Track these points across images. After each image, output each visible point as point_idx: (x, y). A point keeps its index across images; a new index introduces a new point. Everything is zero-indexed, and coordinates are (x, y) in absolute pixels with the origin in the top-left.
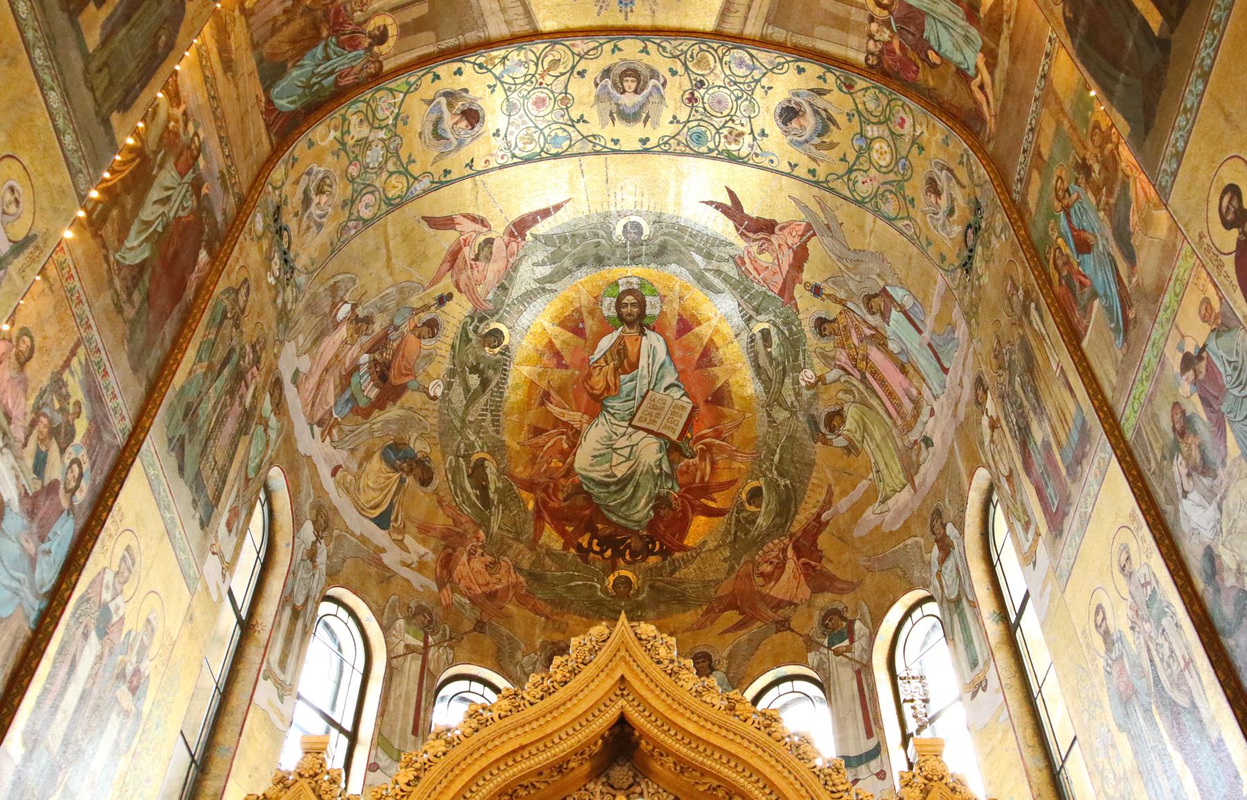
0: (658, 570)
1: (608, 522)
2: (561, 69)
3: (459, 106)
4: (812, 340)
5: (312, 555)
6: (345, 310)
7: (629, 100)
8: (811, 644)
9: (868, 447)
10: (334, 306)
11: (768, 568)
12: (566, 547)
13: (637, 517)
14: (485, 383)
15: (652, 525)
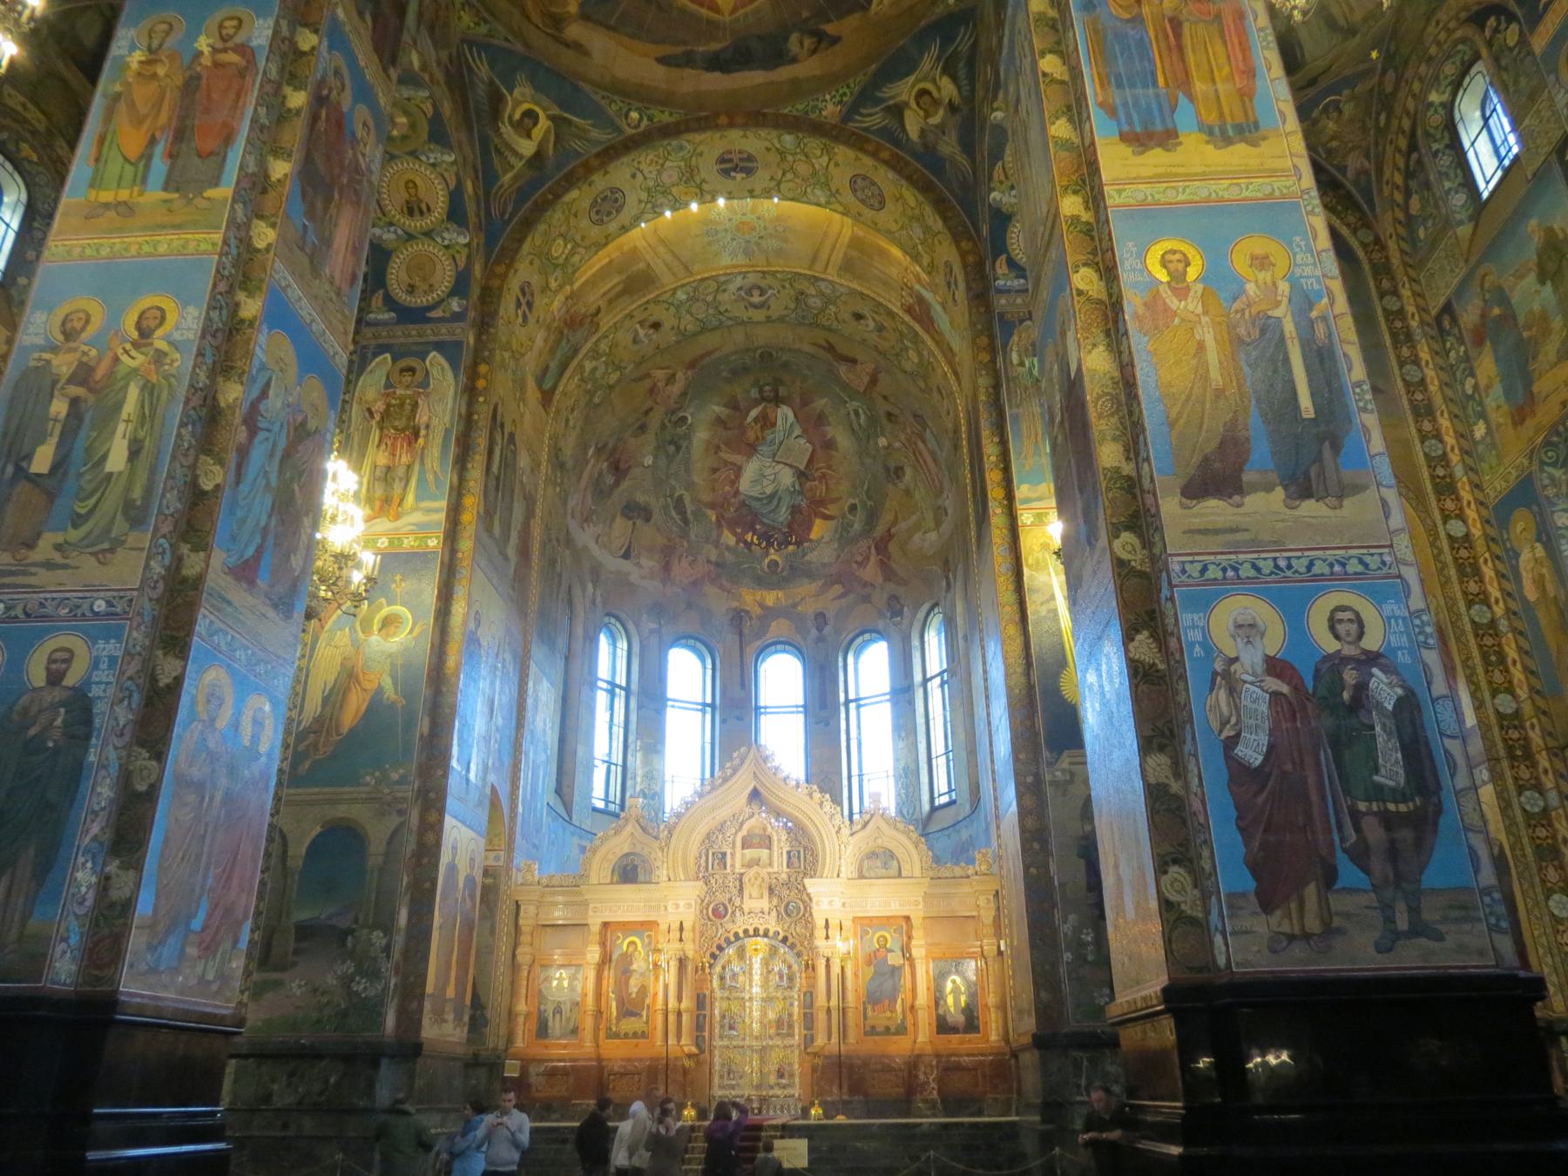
0: (794, 554)
1: (763, 523)
2: (710, 290)
3: (648, 324)
4: (884, 421)
5: (593, 602)
6: (591, 452)
7: (756, 299)
8: (881, 614)
9: (917, 496)
10: (586, 453)
11: (859, 559)
12: (737, 542)
13: (781, 519)
14: (678, 448)
15: (790, 525)
